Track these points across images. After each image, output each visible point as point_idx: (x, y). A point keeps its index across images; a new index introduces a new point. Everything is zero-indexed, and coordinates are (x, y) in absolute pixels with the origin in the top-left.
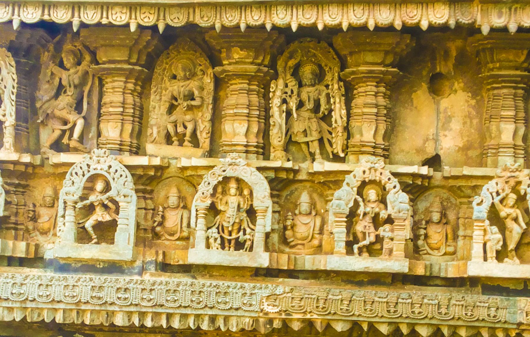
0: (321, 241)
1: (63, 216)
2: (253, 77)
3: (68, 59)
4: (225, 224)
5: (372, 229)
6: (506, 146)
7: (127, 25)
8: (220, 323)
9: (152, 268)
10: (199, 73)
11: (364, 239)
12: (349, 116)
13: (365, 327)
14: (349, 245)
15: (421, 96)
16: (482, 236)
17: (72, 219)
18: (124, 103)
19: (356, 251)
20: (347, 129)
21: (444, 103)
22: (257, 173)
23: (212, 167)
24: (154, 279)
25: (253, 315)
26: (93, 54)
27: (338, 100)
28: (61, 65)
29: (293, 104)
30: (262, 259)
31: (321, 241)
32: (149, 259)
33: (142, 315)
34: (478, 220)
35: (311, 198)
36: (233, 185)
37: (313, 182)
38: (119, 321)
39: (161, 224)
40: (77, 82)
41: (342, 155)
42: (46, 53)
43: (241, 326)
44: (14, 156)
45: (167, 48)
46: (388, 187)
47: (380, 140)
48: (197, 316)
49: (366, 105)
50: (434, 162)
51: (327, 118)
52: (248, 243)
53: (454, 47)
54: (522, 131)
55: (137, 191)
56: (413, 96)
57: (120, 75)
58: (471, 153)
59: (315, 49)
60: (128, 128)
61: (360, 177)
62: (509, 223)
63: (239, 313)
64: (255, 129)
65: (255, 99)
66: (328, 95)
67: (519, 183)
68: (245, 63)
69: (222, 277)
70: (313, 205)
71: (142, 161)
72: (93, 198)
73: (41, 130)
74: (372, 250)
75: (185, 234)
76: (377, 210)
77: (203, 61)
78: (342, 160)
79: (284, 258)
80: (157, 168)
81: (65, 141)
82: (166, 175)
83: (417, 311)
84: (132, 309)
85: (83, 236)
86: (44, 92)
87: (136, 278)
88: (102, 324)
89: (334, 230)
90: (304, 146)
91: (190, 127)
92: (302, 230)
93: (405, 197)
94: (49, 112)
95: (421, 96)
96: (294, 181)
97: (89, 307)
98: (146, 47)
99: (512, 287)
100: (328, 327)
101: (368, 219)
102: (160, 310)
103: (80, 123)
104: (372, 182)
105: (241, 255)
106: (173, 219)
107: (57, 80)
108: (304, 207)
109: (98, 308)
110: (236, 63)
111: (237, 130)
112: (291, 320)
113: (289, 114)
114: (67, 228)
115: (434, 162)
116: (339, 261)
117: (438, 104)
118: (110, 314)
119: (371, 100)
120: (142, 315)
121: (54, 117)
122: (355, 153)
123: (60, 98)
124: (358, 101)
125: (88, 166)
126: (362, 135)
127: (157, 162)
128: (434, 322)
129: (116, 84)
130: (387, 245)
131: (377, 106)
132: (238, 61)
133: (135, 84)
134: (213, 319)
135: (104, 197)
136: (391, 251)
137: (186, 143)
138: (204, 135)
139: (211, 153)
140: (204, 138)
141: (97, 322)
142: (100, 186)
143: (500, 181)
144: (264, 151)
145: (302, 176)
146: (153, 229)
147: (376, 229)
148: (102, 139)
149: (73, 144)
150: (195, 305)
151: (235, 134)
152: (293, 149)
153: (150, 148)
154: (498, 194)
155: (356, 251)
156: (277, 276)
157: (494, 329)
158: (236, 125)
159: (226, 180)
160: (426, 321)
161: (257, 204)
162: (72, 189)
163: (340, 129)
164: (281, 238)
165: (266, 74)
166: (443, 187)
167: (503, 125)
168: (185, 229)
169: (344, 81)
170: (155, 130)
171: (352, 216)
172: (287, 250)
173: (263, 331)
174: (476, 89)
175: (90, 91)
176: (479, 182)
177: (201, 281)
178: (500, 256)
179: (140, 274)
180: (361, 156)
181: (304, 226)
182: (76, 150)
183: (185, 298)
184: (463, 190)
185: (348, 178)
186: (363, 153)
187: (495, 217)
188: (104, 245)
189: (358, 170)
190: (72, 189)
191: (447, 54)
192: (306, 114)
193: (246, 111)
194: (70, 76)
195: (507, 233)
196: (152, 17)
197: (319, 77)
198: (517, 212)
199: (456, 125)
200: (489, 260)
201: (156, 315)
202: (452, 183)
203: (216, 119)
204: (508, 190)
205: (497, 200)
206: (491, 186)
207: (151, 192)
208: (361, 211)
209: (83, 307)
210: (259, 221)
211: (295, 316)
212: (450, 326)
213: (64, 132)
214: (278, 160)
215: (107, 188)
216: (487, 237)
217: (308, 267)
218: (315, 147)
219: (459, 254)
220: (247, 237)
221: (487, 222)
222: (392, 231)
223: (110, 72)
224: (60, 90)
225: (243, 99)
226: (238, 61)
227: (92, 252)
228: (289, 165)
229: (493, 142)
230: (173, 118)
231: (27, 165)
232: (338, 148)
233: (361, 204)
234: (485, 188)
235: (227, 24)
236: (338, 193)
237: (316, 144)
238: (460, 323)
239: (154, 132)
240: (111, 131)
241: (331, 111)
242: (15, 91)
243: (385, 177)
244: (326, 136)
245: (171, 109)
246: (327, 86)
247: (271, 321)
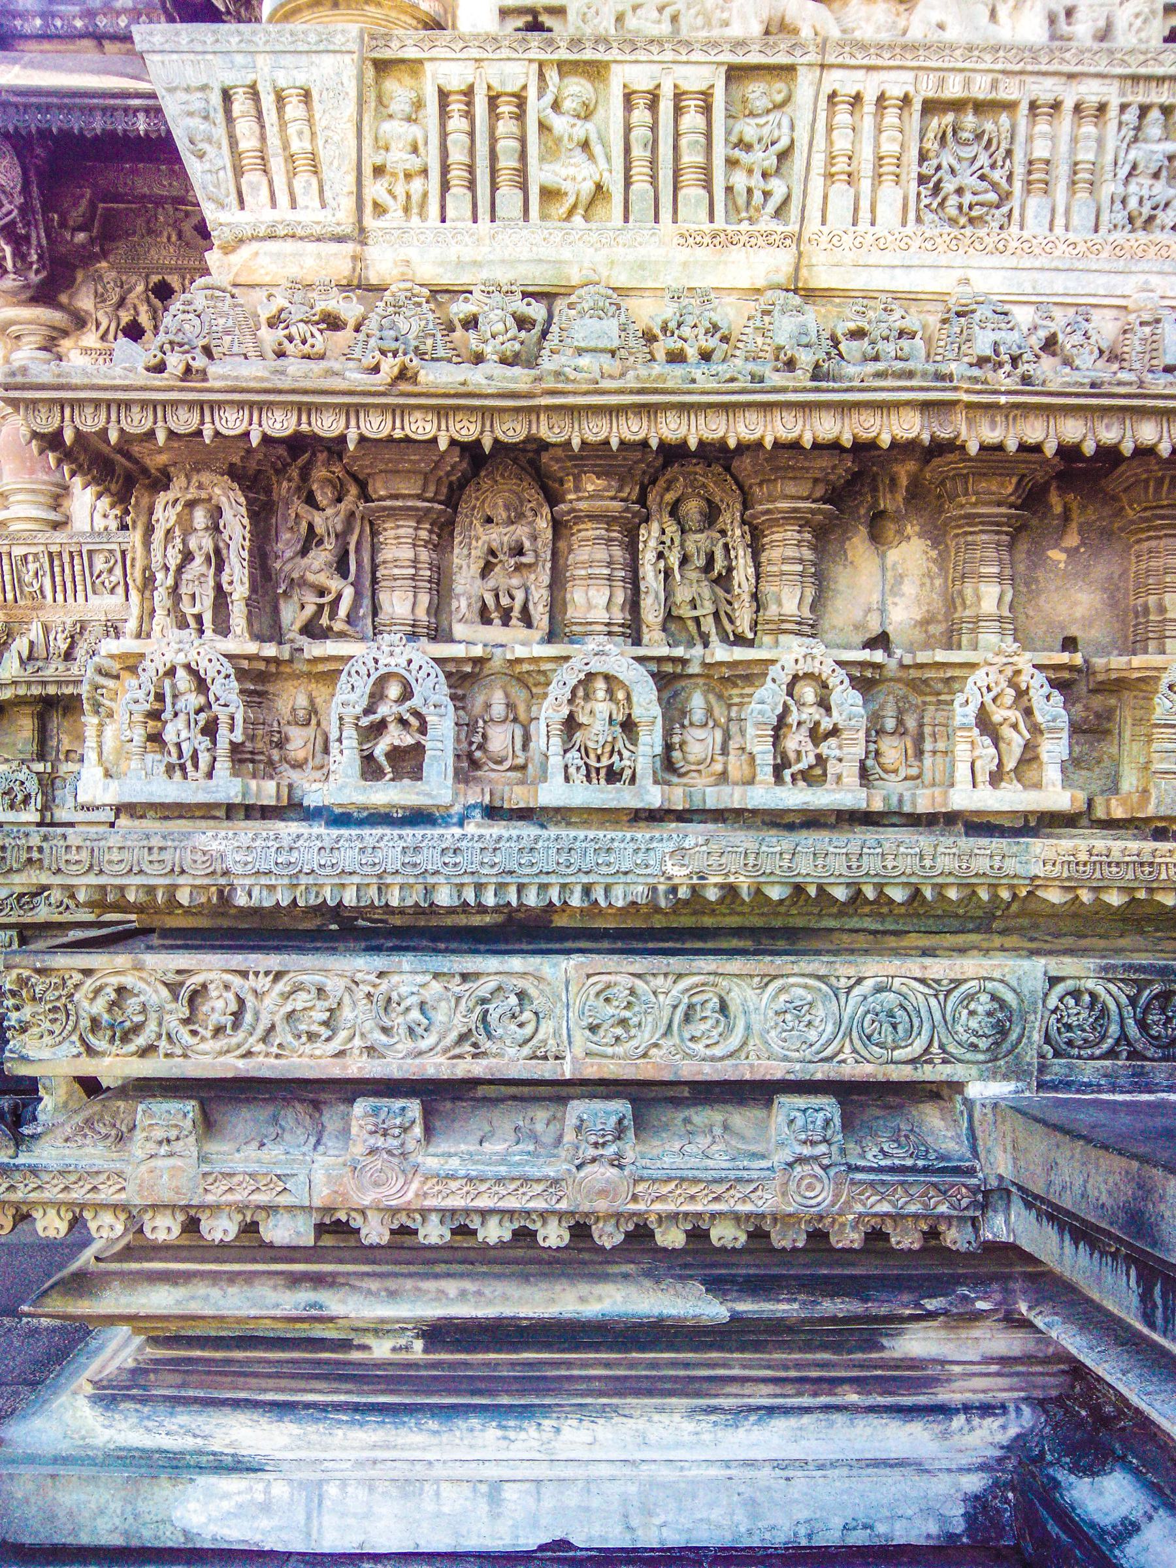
0: (725, 764)
1: (340, 740)
2: (615, 519)
3: (324, 494)
4: (591, 745)
5: (810, 746)
6: (988, 618)
7: (434, 440)
8: (598, 894)
9: (477, 813)
10: (529, 514)
11: (798, 760)
12: (758, 577)
13: (812, 891)
14: (778, 771)
15: (859, 546)
16: (970, 750)
17: (355, 744)
18: (415, 561)
19: (788, 778)
20: (755, 596)
21: (893, 555)
22: (636, 665)
23: (567, 659)
24: (483, 831)
25: (650, 880)
26: (362, 485)
27: (741, 553)
28: (311, 500)
29: (674, 559)
30: (653, 797)
31: (725, 764)
32: (472, 801)
33: (479, 888)
34: (963, 727)
35: (707, 702)
36: (600, 685)
37: (708, 676)
38: (444, 897)
39: (481, 747)
40: (339, 528)
41: (750, 636)
42: (285, 484)
43: (630, 898)
44: (252, 648)
45: (476, 474)
46: (831, 682)
47: (806, 613)
48: (564, 886)
49: (785, 560)
50: (881, 641)
51: (724, 581)
52: (627, 773)
53: (904, 471)
54: (1008, 597)
55: (453, 697)
56: (847, 545)
57: (408, 517)
58: (932, 629)
59: (705, 475)
60: (424, 599)
61: (791, 669)
62: (1006, 732)
63: (629, 879)
64: (620, 597)
65: (618, 553)
66: (726, 546)
67: (1018, 672)
68: (602, 498)
69: (586, 824)
70: (709, 711)
71: (458, 651)
72: (383, 710)
73: (282, 605)
74: (813, 776)
75: (520, 761)
76: (817, 717)
77: (533, 495)
78: (750, 643)
79: (678, 792)
80: (478, 661)
81: (324, 621)
82: (486, 672)
83: (890, 865)
84: (466, 879)
85: (370, 768)
86: (286, 544)
87: (457, 831)
88: (417, 905)
89: (755, 750)
90: (690, 623)
91: (520, 596)
92: (696, 750)
93: (856, 697)
94: (295, 575)
95: (859, 546)
96: (681, 676)
97: (399, 879)
98: (448, 474)
99: (1007, 824)
100: (758, 891)
101: (804, 731)
102: (508, 879)
103: (348, 593)
104: (808, 676)
105: (618, 791)
106: (500, 739)
107: (304, 526)
108: (698, 715)
109: (412, 880)
110: (591, 497)
111: (593, 601)
112: (704, 886)
113: (668, 574)
114: (345, 758)
115: (881, 641)
116: (765, 795)
117: (883, 556)
118: (429, 890)
119: (791, 552)
120: (479, 888)
121: (303, 583)
122: (771, 632)
123: (312, 554)
124: (772, 554)
125: (376, 661)
126: (780, 605)
127: (477, 651)
128: (913, 880)
129: (401, 531)
130: (832, 768)
131: (801, 561)
132: (591, 492)
133: (431, 532)
134: (587, 890)
135: (403, 709)
136: (839, 777)
137: (514, 622)
138: (541, 609)
139: (551, 637)
140: (540, 613)
141: (409, 902)
142: (394, 691)
143: (991, 669)
144: (633, 632)
145: (694, 669)
146: (470, 755)
147: (816, 745)
148: (382, 617)
149: (338, 626)
150: (562, 869)
151: (590, 606)
152: (673, 627)
153: (459, 630)
154: (989, 689)
155: (788, 778)
156: (662, 820)
157: (995, 886)
158: (592, 592)
159: (590, 676)
160: (904, 879)
161: (637, 713)
162: (353, 697)
163: (746, 597)
164: (668, 765)
165: (635, 514)
166: (899, 680)
167: (983, 588)
168: (519, 753)
169: (750, 524)
170: (464, 603)
171: (780, 727)
172: (675, 780)
173: (663, 904)
174: (936, 536)
175: (358, 543)
176: (957, 673)
177: (553, 832)
178: (996, 778)
179: (461, 824)
180: (783, 638)
181: (699, 743)
182: (342, 635)
183: (547, 859)
184: (930, 686)
185: (773, 671)
186: (785, 631)
187: (985, 724)
188: (406, 781)
189: (787, 659)
190: (353, 697)
191: (893, 482)
192: (694, 575)
193: (607, 571)
194: (327, 520)
195: (1002, 745)
196: (472, 427)
197: (711, 515)
198: (1015, 715)
199: (910, 588)
200: (980, 786)
201: (501, 887)
202: (913, 673)
203: (557, 583)
204: (1004, 684)
205: (988, 698)
206: (979, 677)
207: (462, 698)
208: (793, 719)
209: (389, 880)
210: (643, 738)
211: (713, 880)
212: (934, 885)
213: (321, 607)
214: (656, 645)
215: (407, 693)
216: (977, 753)
217: (711, 804)
218: (709, 625)
219: (928, 777)
220: (626, 762)
221: (976, 731)
222: (840, 747)
223: (393, 513)
224: (311, 540)
225: (601, 554)
226: (591, 492)
227: (388, 794)
228: (679, 652)
229: (968, 613)
230: (491, 583)
231: (267, 660)
232: (743, 624)
233: (794, 708)
234: (970, 681)
235: (591, 438)
236: (760, 693)
237: (710, 619)
238: (951, 880)
239: (461, 605)
240: (398, 604)
241: (730, 569)
242: (247, 544)
243: (826, 670)
244: (725, 607)
245: (486, 570)
246: (723, 533)
247: (674, 890)
